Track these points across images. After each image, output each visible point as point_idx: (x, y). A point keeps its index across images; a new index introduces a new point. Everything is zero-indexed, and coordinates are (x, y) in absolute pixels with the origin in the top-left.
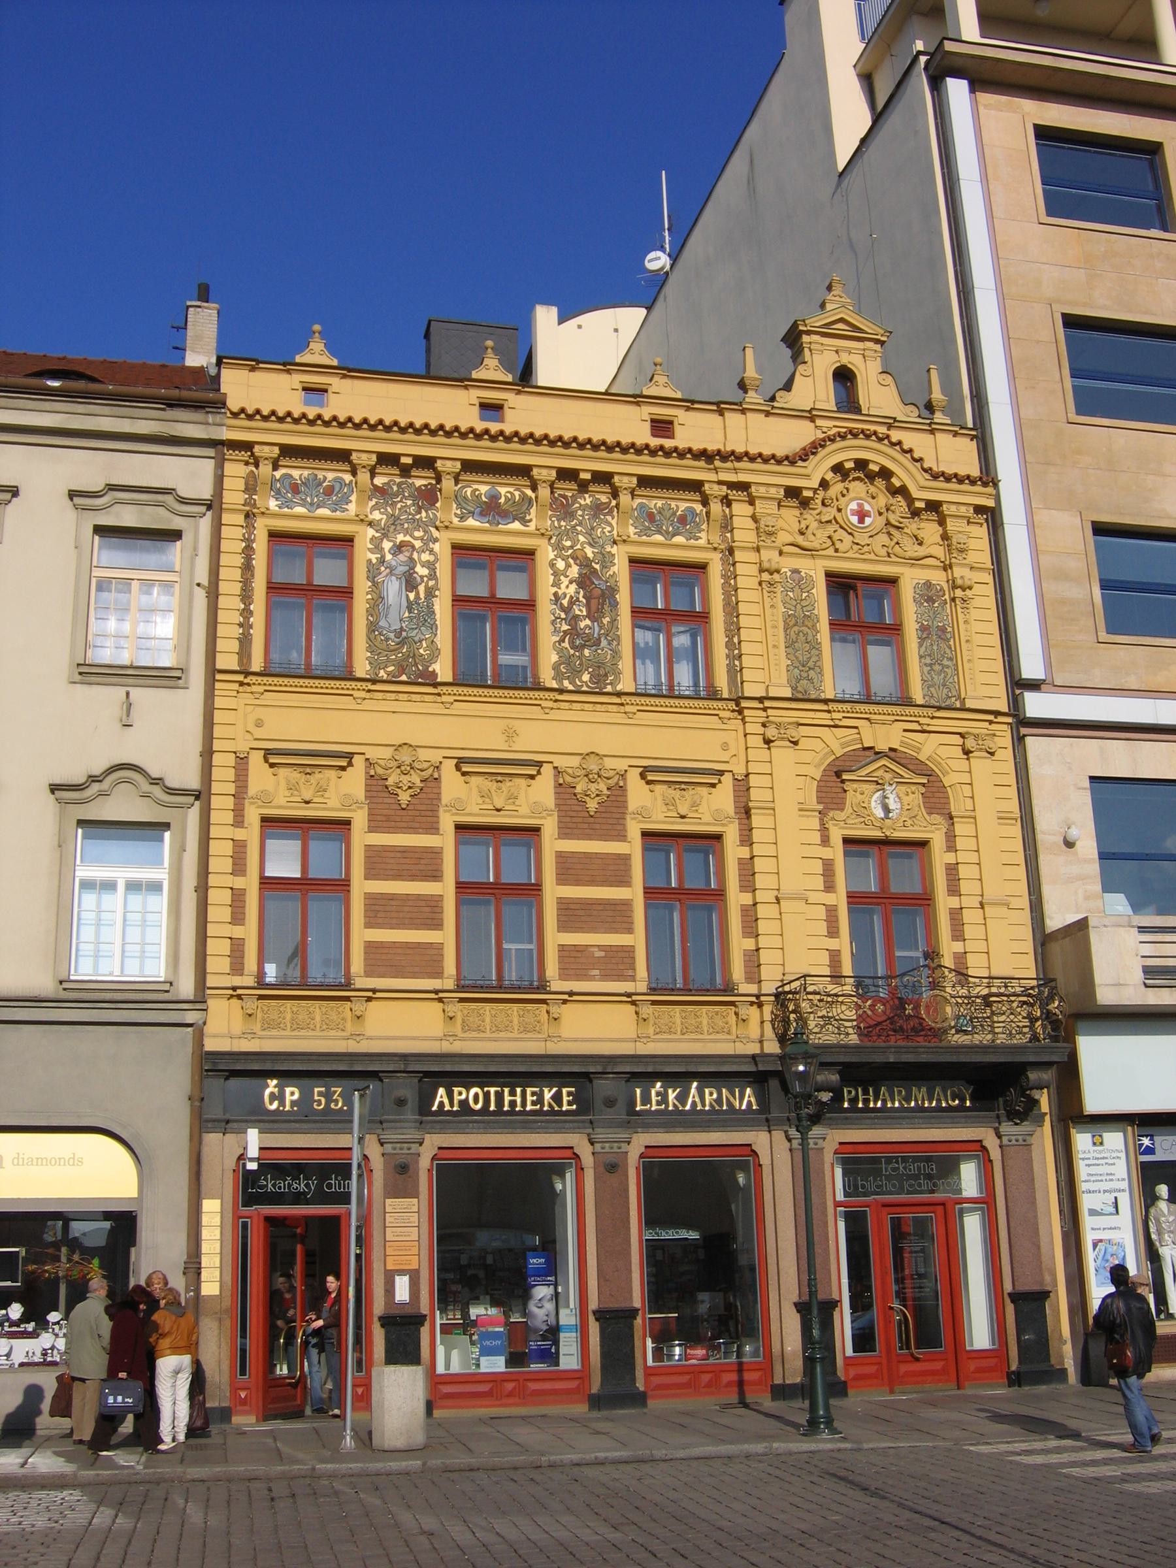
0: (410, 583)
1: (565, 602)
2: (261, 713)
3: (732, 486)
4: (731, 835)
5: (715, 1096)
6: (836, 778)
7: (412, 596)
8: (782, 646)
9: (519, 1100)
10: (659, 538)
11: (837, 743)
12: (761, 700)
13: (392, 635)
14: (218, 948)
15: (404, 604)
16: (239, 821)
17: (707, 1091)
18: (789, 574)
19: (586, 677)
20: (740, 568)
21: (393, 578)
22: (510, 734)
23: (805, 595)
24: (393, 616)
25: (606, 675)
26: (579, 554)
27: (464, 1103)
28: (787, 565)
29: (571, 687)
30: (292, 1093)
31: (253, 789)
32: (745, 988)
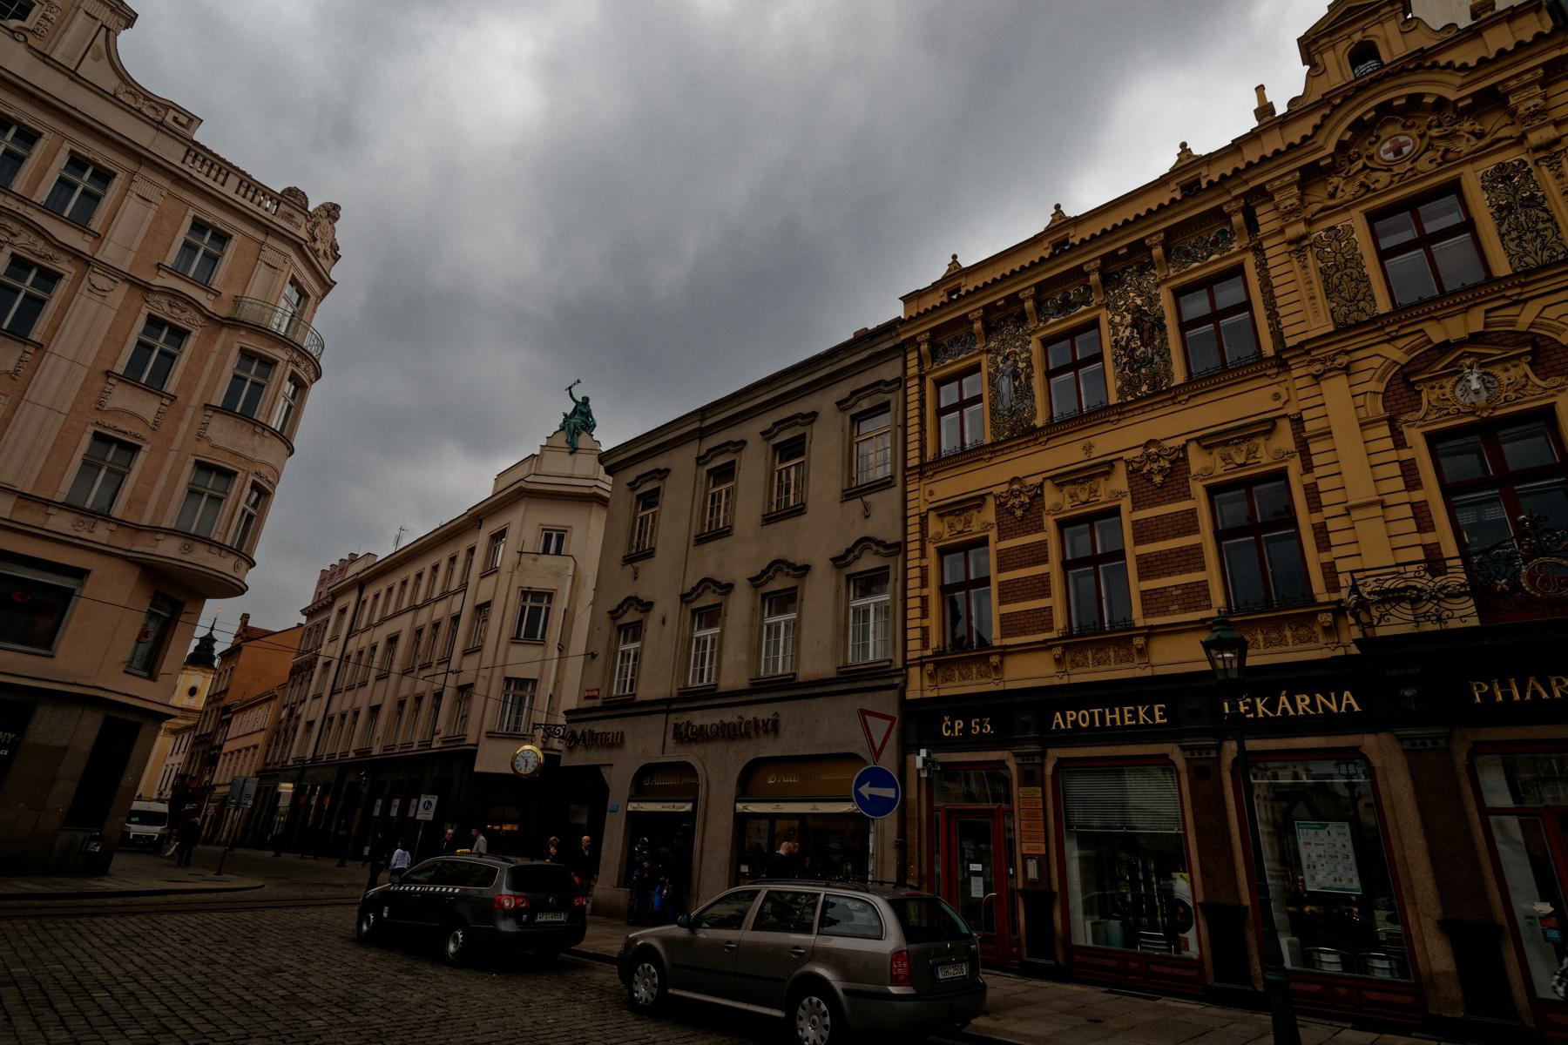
0: (1015, 375)
3: (1245, 195)
4: (1294, 467)
5: (1308, 701)
6: (1402, 389)
9: (1117, 716)
11: (1395, 354)
12: (1301, 345)
14: (914, 634)
16: (923, 556)
17: (1298, 698)
19: (1144, 388)
22: (1088, 448)
24: (1006, 399)
27: (1075, 723)
28: (1319, 231)
30: (959, 724)
31: (932, 531)
32: (1323, 597)
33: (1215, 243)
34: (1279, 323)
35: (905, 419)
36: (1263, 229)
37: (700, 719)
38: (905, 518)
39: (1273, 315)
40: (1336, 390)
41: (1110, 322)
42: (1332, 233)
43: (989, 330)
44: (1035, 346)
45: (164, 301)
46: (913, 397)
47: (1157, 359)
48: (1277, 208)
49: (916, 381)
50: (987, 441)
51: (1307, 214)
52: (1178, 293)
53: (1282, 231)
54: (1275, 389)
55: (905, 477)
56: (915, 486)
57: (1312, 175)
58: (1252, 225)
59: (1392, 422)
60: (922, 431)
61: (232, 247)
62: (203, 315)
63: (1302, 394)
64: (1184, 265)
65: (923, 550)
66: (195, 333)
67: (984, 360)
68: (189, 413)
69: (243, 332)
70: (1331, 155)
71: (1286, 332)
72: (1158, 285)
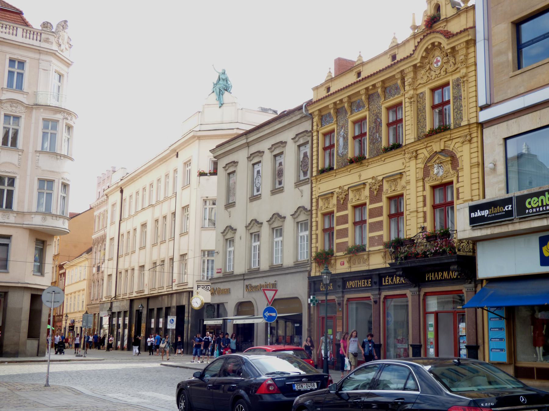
0: (344, 138)
37: (255, 283)
38: (312, 199)
45: (8, 105)
59: (423, 179)
61: (27, 66)
62: (23, 106)
65: (317, 214)
66: (23, 116)
68: (30, 155)
69: (42, 110)
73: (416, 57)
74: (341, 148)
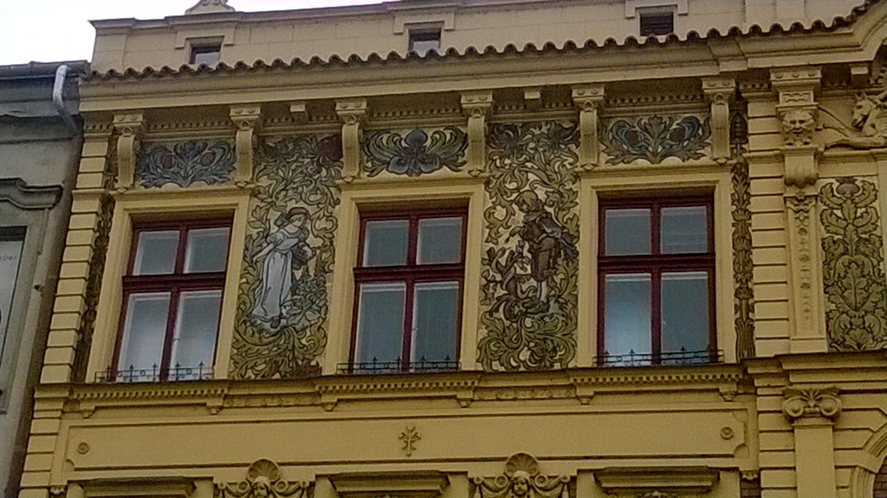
0: (298, 259)
1: (503, 261)
2: (85, 436)
3: (740, 76)
7: (298, 274)
8: (817, 285)
10: (642, 163)
12: (777, 359)
13: (267, 325)
15: (288, 284)
18: (836, 185)
19: (525, 355)
20: (755, 187)
21: (278, 255)
22: (410, 439)
23: (860, 211)
24: (272, 299)
25: (554, 350)
26: (527, 197)
28: (831, 175)
29: (502, 369)
33: (678, 135)
34: (750, 309)
35: (55, 279)
36: (754, 144)
39: (744, 292)
40: (814, 442)
41: (488, 214)
42: (847, 187)
43: (264, 150)
44: (346, 214)
46: (81, 236)
47: (554, 307)
48: (779, 116)
49: (95, 205)
50: (221, 374)
51: (819, 142)
52: (608, 201)
53: (780, 158)
54: (729, 420)
55: (30, 403)
56: (51, 426)
57: (837, 80)
58: (739, 133)
60: (89, 315)
63: (766, 441)
64: (624, 156)
67: (244, 209)
70: (869, 63)
71: (760, 330)
72: (577, 177)
73: (858, 38)
74: (272, 299)
